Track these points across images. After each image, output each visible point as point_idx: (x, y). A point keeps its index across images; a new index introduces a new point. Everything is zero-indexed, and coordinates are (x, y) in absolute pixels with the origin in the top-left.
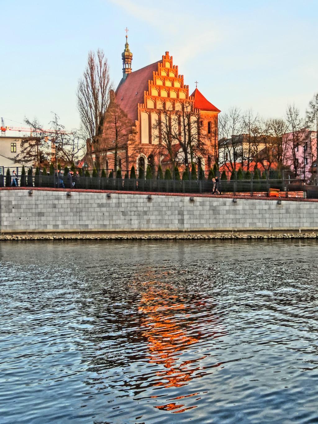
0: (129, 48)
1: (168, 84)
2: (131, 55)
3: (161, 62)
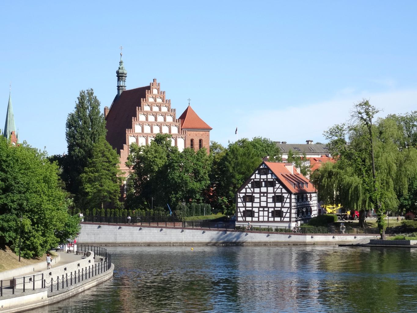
0: (123, 65)
1: (155, 109)
2: (125, 72)
3: (148, 88)
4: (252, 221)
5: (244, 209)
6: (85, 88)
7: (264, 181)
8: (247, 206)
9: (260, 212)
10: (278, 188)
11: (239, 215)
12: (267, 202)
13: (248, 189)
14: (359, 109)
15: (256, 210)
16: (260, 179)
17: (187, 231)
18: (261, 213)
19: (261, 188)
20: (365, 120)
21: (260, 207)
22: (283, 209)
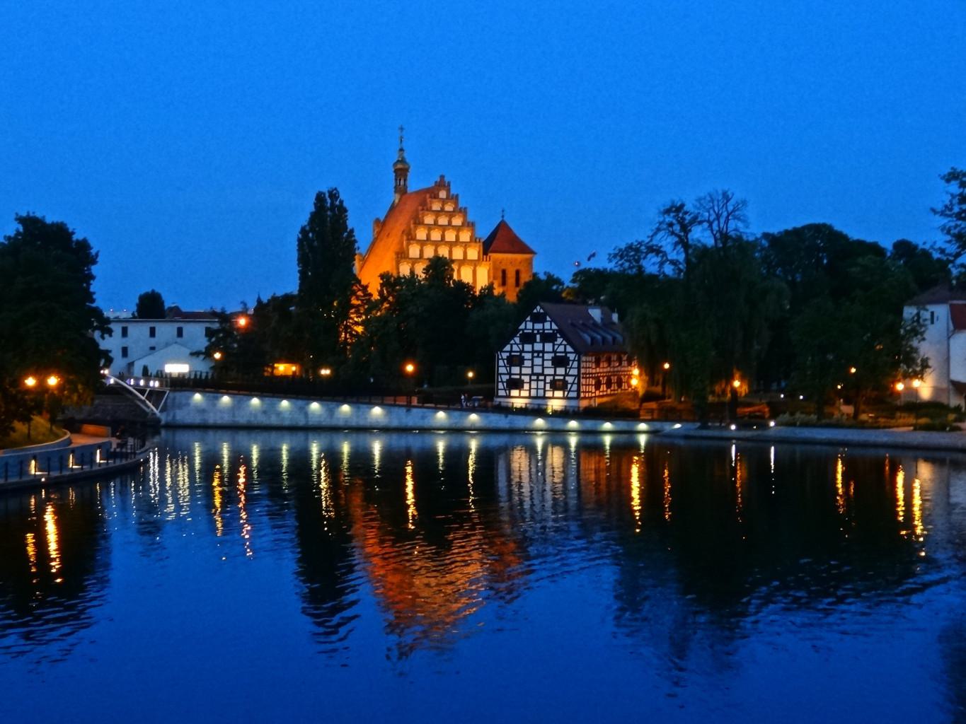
0: (406, 155)
1: (443, 221)
4: (519, 397)
5: (507, 377)
6: (325, 189)
7: (538, 333)
8: (513, 372)
9: (532, 382)
10: (561, 344)
11: (501, 386)
12: (543, 365)
13: (515, 346)
14: (668, 219)
15: (526, 379)
16: (533, 329)
17: (414, 410)
18: (534, 385)
19: (535, 344)
20: (679, 236)
21: (533, 374)
22: (567, 378)
